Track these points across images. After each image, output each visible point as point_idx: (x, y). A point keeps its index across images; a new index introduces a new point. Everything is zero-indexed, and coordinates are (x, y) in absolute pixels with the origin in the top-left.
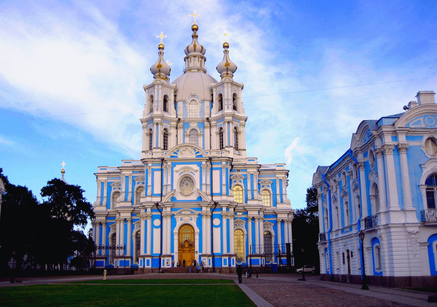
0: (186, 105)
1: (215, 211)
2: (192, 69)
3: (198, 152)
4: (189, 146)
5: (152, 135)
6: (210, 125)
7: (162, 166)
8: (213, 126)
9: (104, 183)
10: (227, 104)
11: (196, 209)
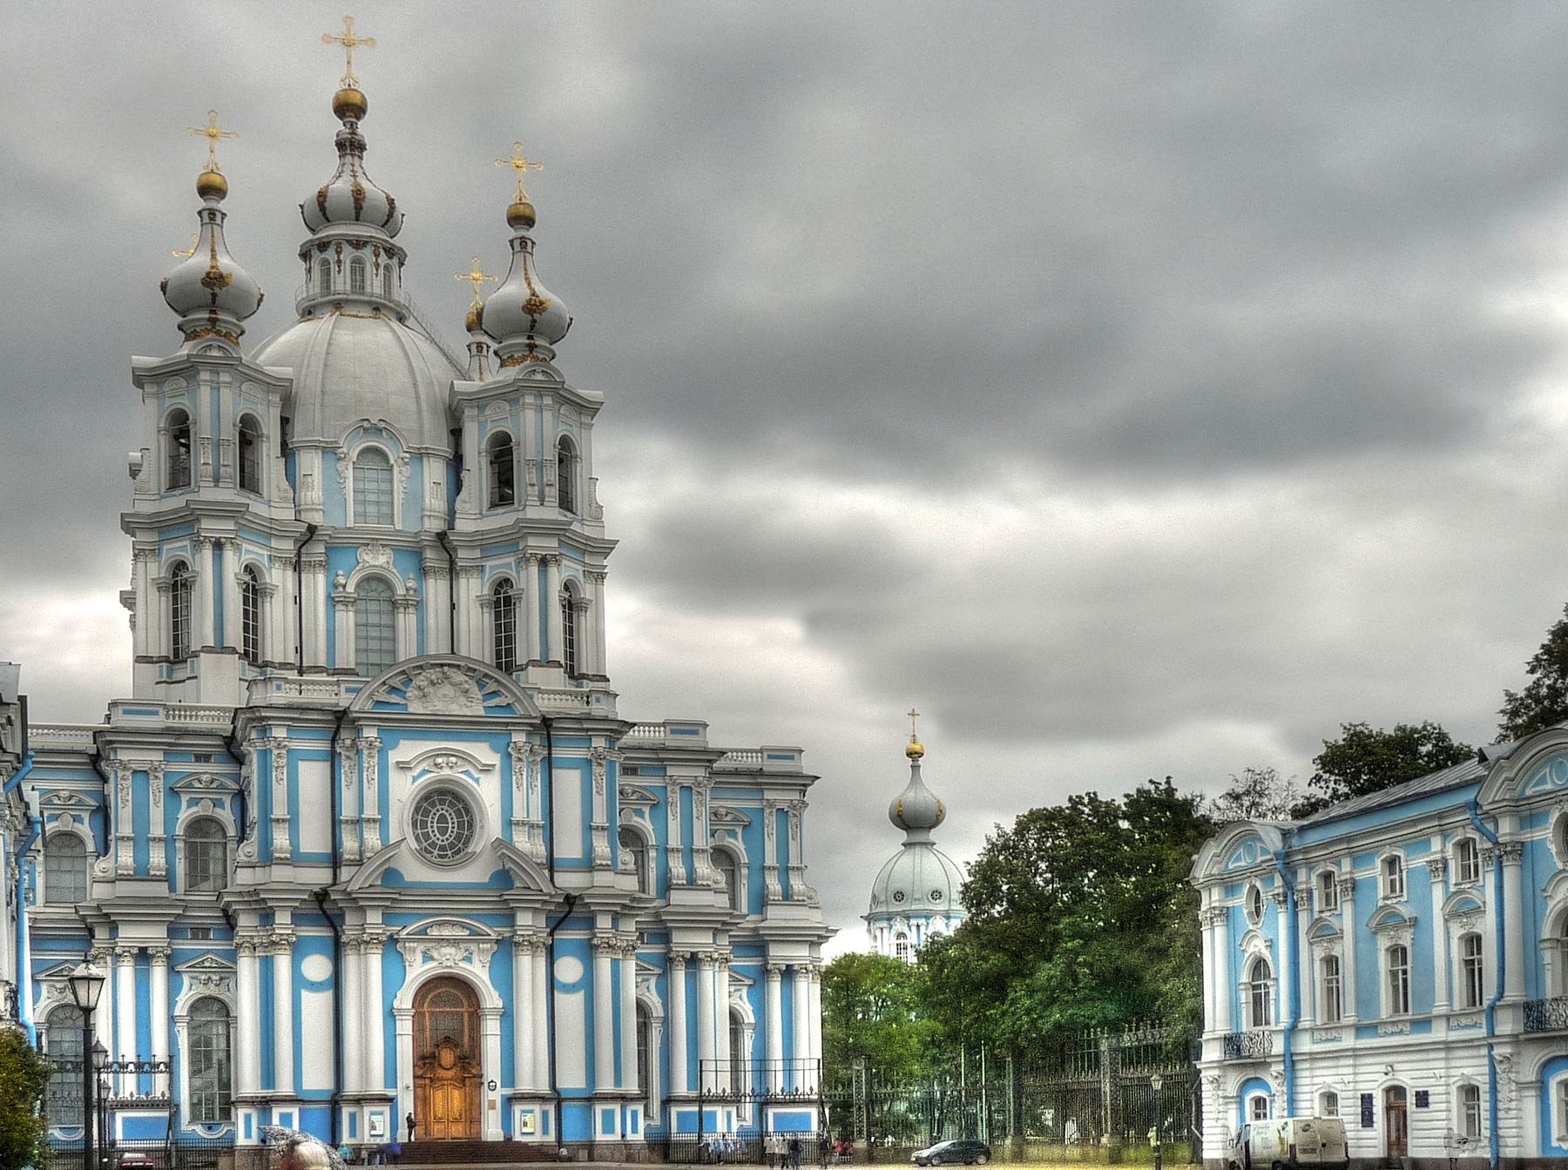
0: (340, 466)
2: (347, 301)
3: (495, 694)
4: (459, 666)
5: (184, 585)
10: (534, 481)
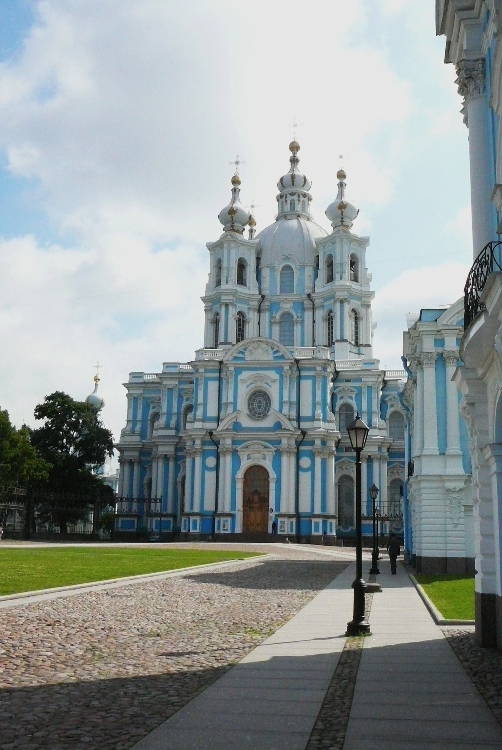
0: (275, 273)
1: (303, 445)
2: (288, 215)
6: (314, 305)
8: (319, 307)
9: (137, 398)
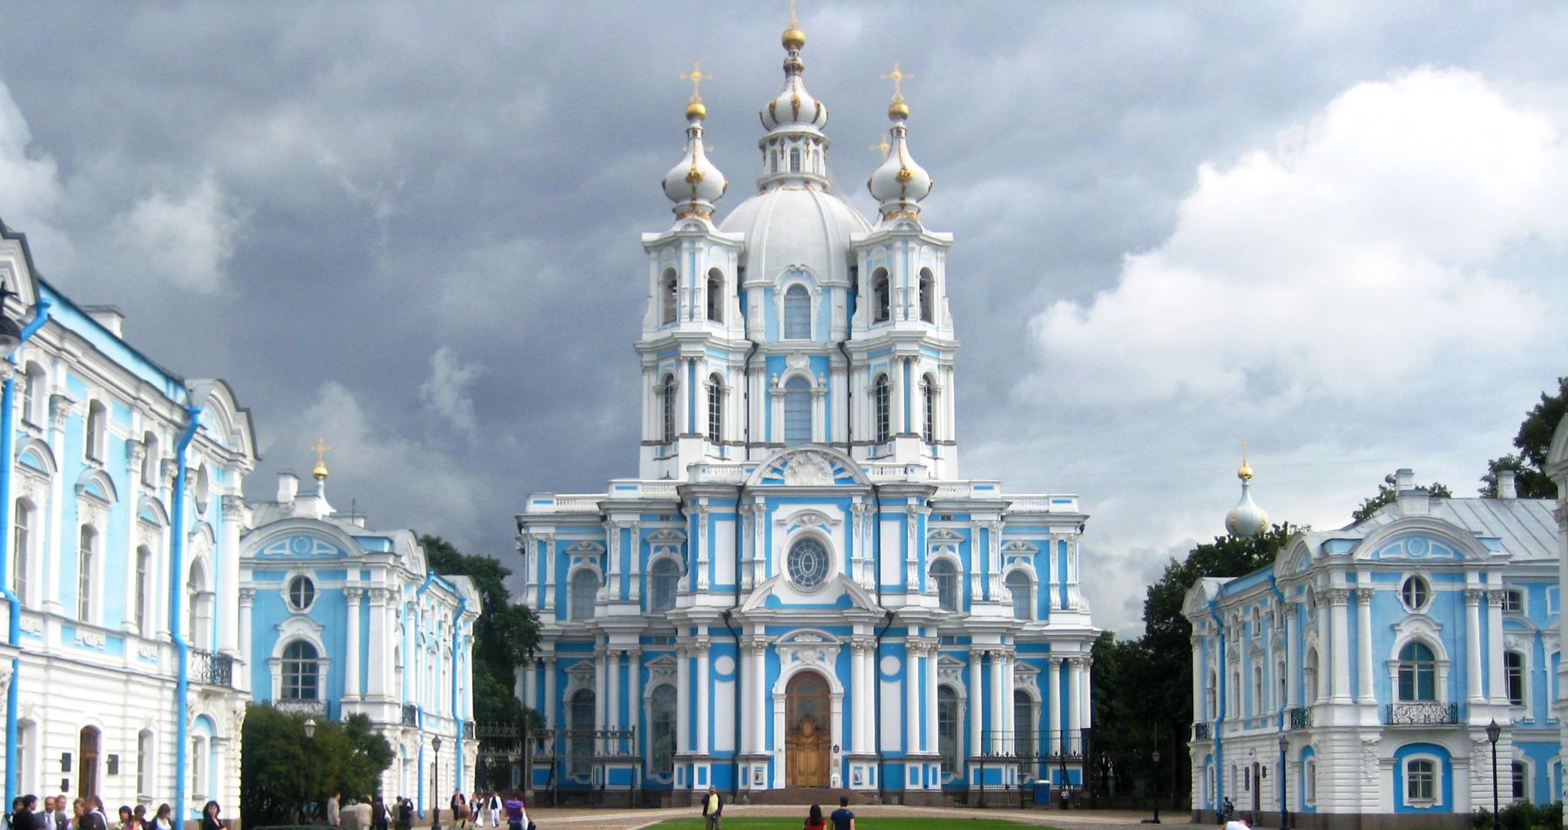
0: (775, 299)
1: (888, 635)
3: (841, 470)
5: (672, 389)
7: (737, 507)
8: (859, 368)
9: (545, 543)
11: (836, 630)
